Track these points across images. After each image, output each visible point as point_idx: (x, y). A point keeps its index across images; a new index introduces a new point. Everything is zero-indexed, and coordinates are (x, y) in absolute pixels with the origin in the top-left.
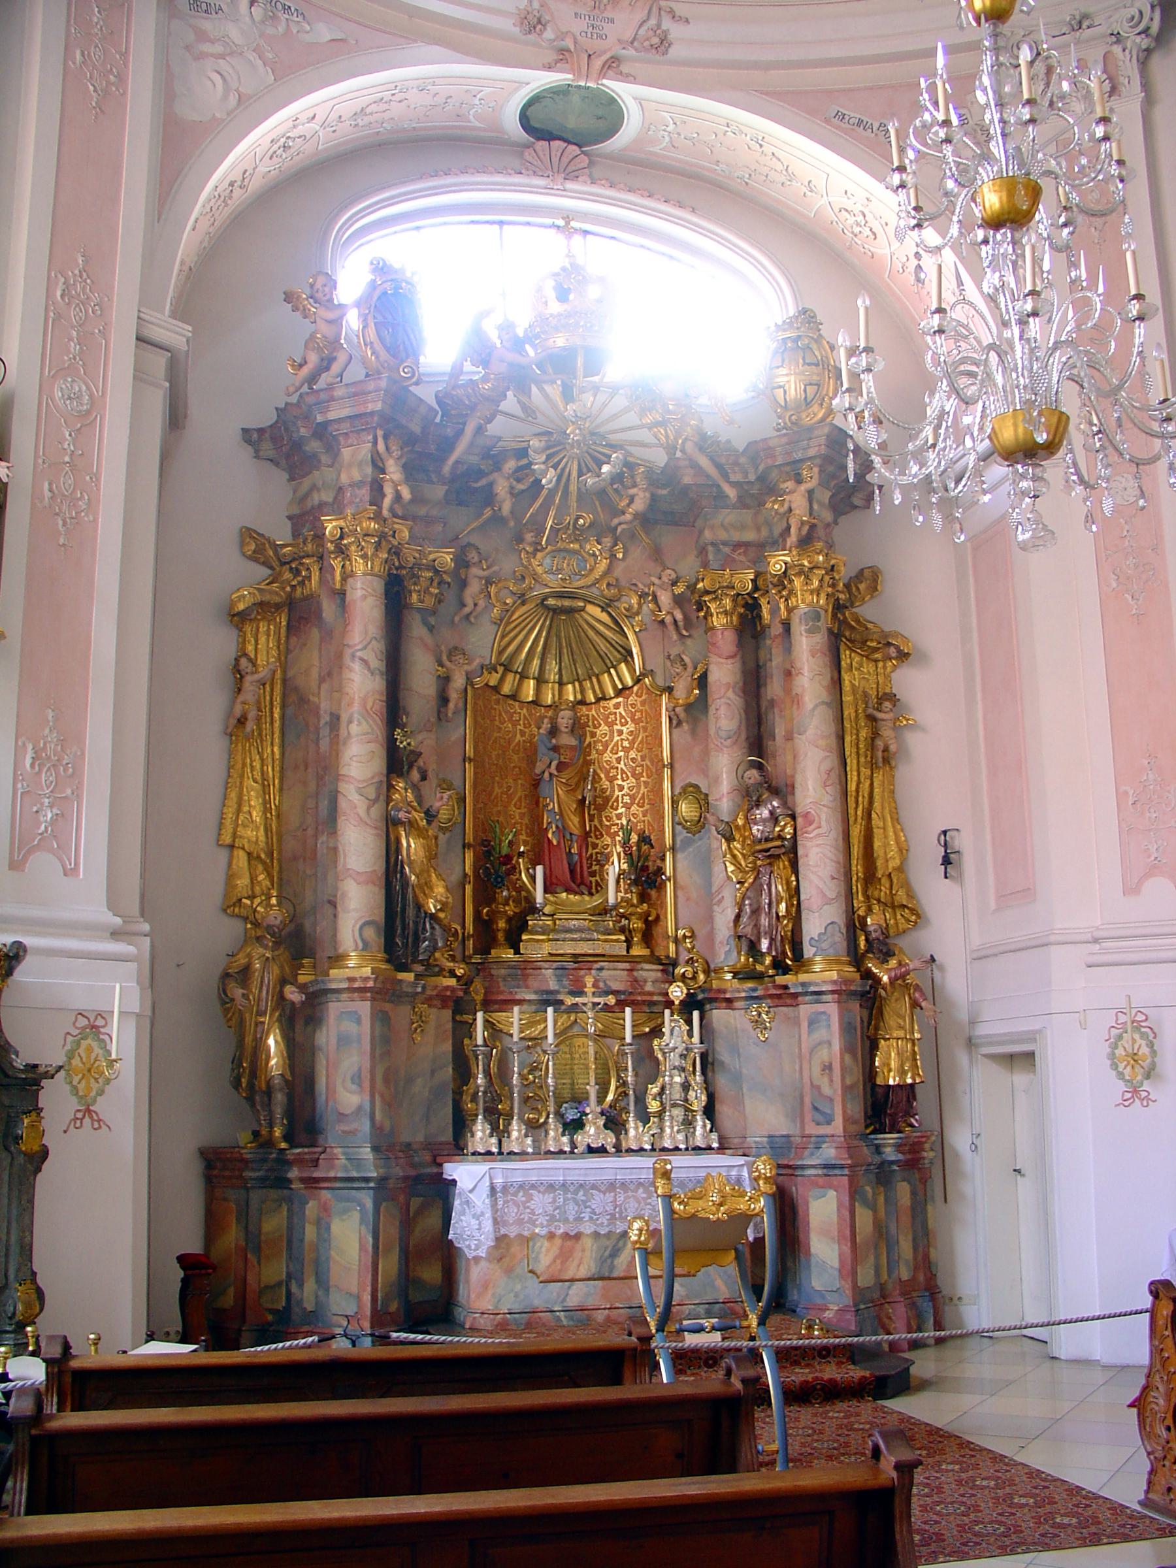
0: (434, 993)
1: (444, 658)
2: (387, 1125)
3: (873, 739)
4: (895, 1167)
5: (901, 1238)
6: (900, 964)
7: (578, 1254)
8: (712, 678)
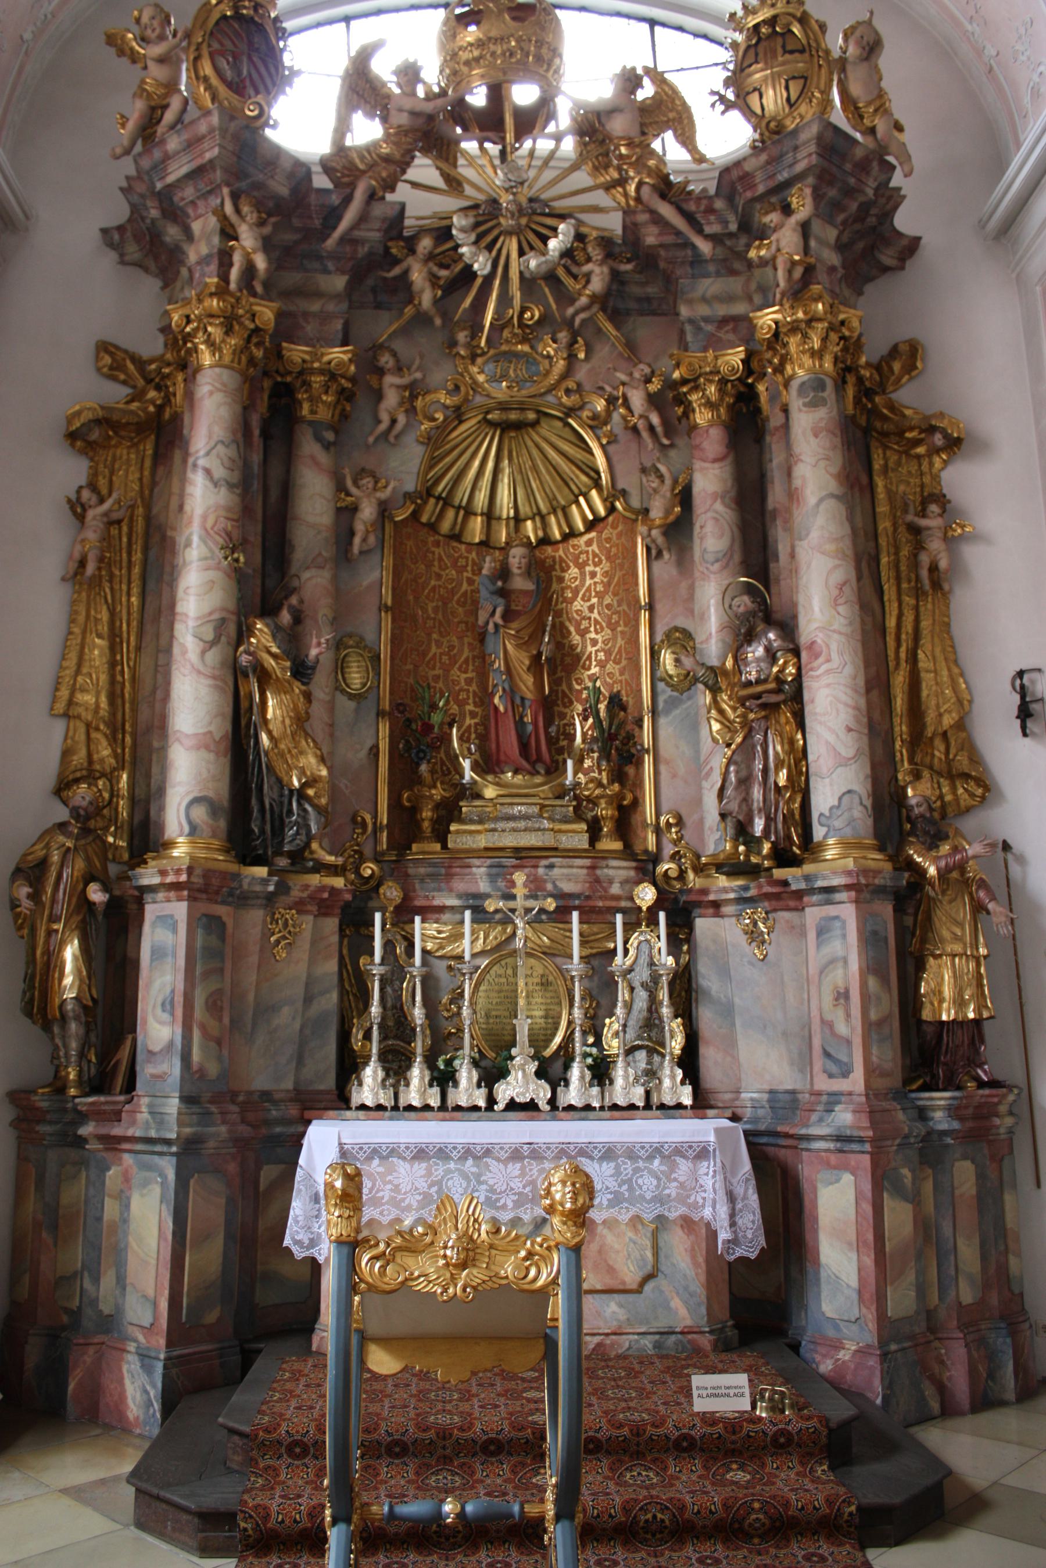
0: (305, 895)
1: (349, 483)
3: (916, 556)
5: (960, 1243)
6: (956, 849)
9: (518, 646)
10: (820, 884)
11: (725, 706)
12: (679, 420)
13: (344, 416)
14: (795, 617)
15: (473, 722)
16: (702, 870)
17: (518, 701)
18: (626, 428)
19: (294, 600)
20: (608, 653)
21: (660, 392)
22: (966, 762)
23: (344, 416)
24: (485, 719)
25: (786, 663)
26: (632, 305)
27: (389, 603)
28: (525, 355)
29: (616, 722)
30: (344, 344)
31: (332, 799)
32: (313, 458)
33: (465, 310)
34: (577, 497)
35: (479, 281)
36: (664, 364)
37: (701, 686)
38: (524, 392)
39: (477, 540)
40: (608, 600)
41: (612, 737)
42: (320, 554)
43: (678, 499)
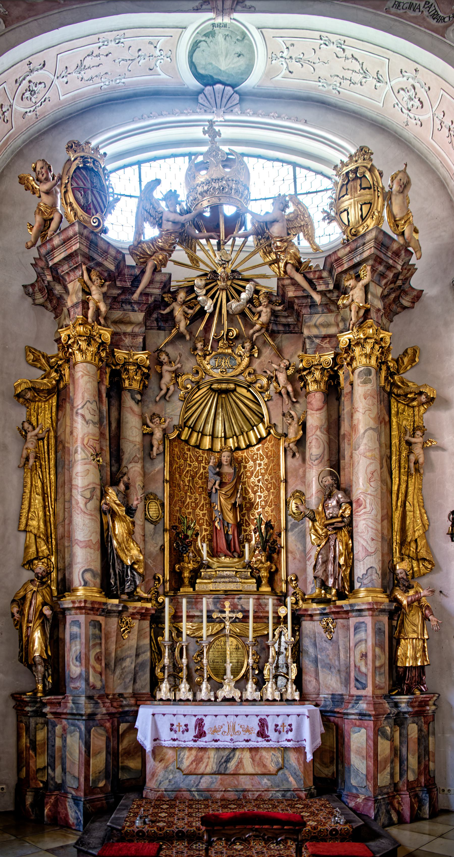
2: (98, 685)
3: (408, 456)
4: (407, 716)
6: (417, 592)
7: (205, 760)
8: (308, 425)
9: (226, 499)
10: (356, 608)
11: (317, 528)
12: (301, 388)
13: (145, 387)
14: (351, 486)
18: (276, 393)
21: (293, 375)
22: (425, 553)
23: (145, 387)
25: (346, 508)
26: (281, 328)
28: (230, 354)
30: (144, 349)
32: (131, 408)
34: (253, 427)
35: (207, 315)
36: (295, 360)
38: (229, 375)
43: (301, 427)
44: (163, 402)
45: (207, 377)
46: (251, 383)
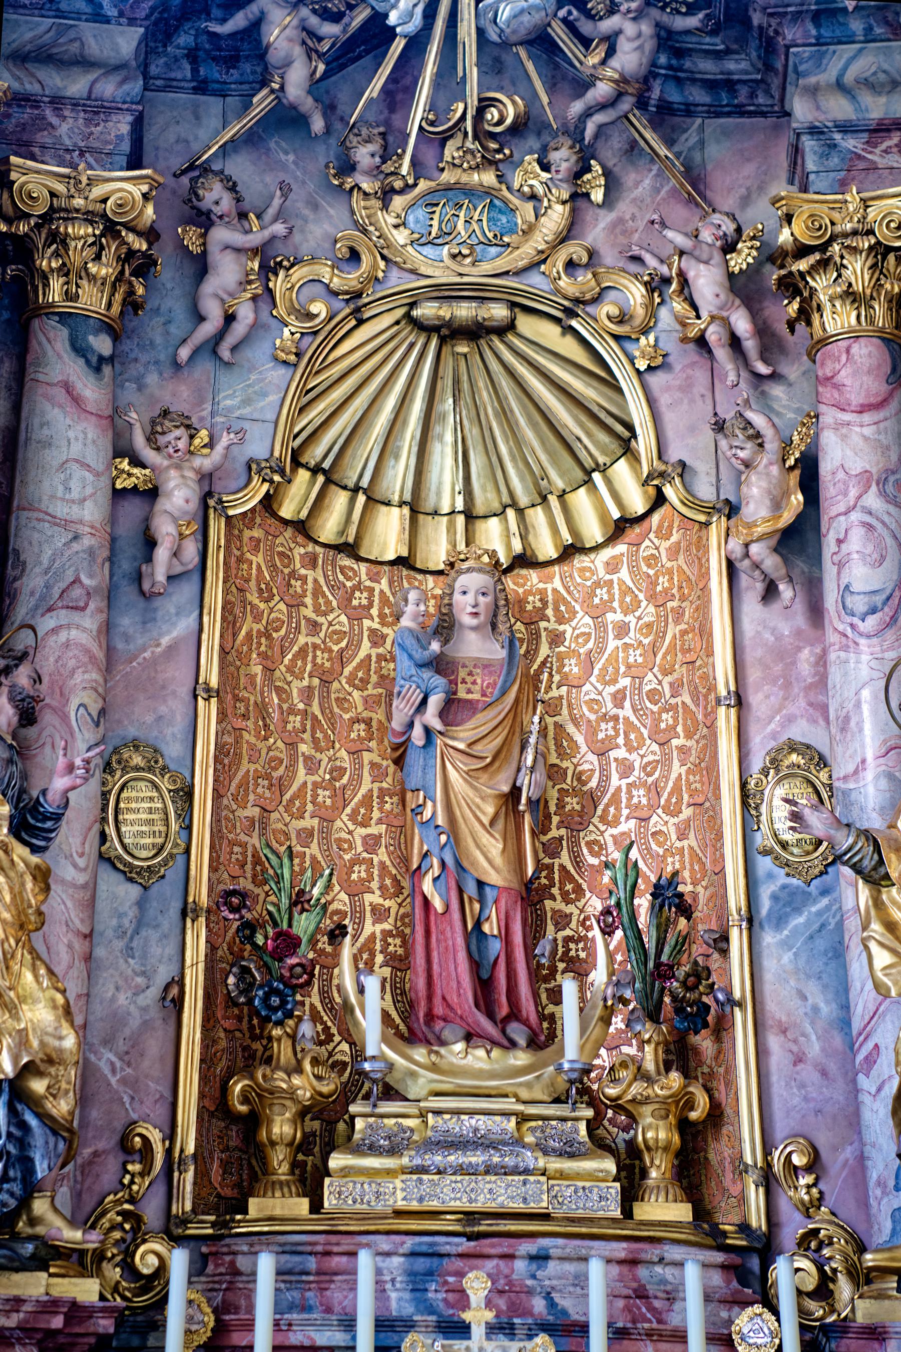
1: (139, 441)
8: (826, 467)
9: (470, 775)
12: (791, 325)
15: (379, 928)
16: (868, 1282)
17: (471, 889)
18: (684, 340)
19: (22, 676)
20: (655, 790)
21: (753, 272)
23: (132, 305)
24: (406, 919)
26: (699, 96)
27: (214, 682)
28: (488, 192)
29: (671, 939)
30: (135, 162)
31: (83, 1100)
32: (68, 388)
33: (371, 101)
34: (588, 473)
35: (398, 46)
37: (846, 871)
38: (486, 267)
39: (391, 556)
40: (650, 682)
41: (663, 972)
42: (77, 581)
44: (206, 365)
45: (395, 273)
46: (577, 301)
